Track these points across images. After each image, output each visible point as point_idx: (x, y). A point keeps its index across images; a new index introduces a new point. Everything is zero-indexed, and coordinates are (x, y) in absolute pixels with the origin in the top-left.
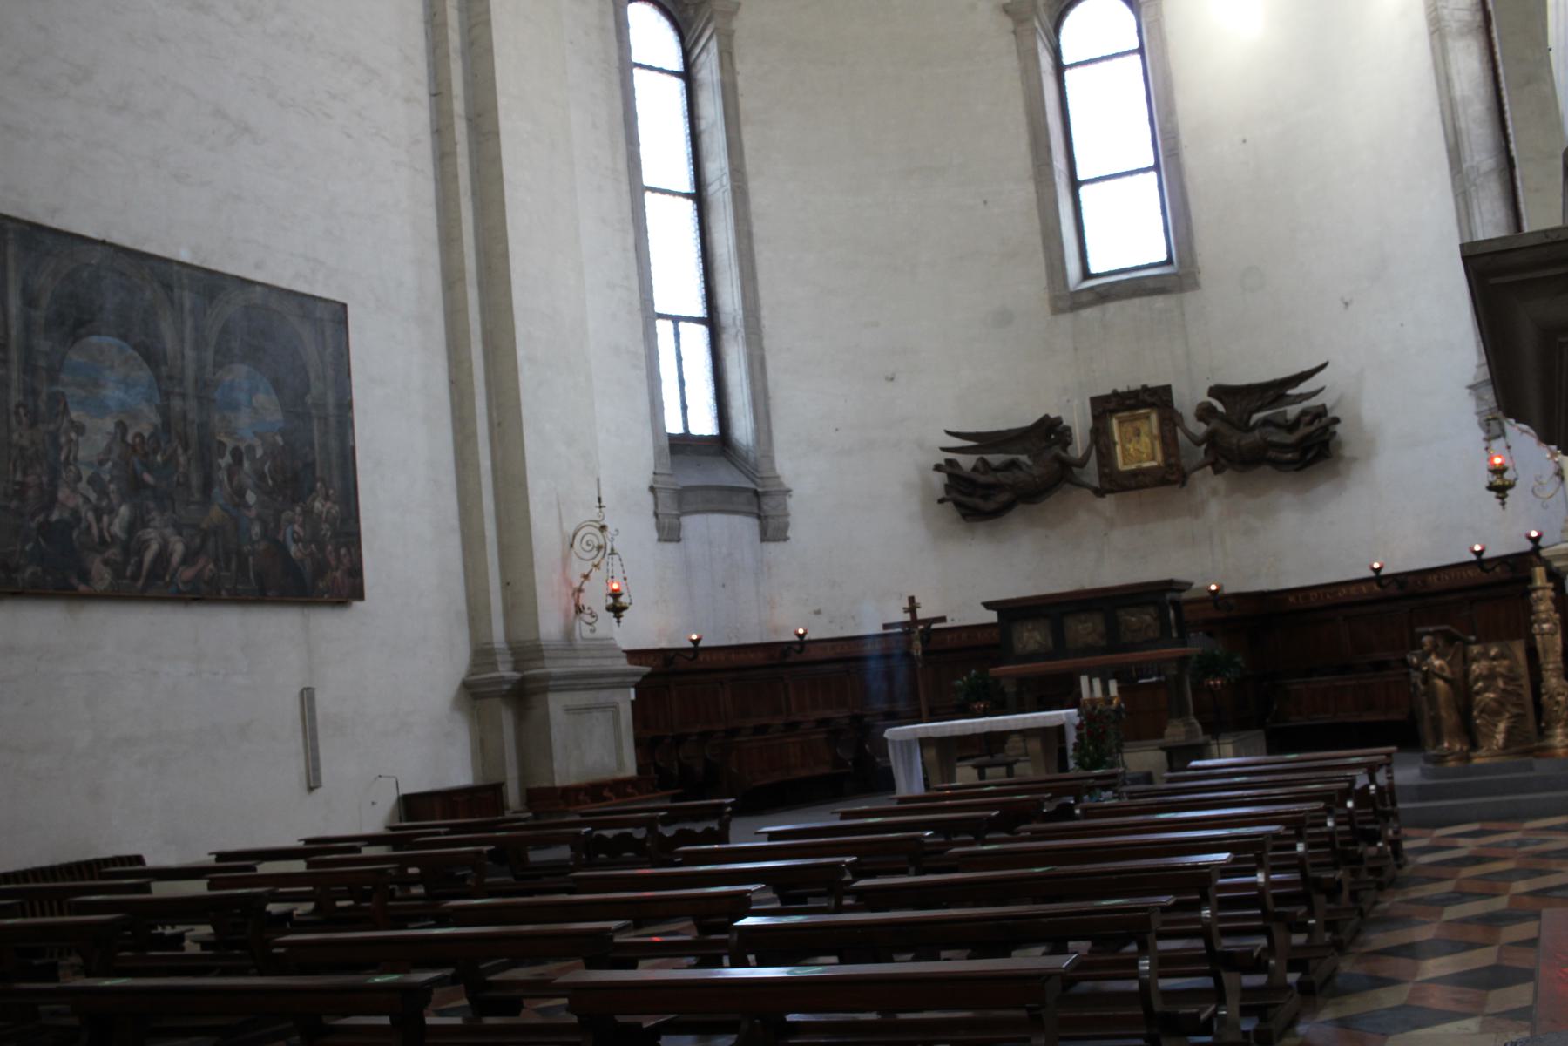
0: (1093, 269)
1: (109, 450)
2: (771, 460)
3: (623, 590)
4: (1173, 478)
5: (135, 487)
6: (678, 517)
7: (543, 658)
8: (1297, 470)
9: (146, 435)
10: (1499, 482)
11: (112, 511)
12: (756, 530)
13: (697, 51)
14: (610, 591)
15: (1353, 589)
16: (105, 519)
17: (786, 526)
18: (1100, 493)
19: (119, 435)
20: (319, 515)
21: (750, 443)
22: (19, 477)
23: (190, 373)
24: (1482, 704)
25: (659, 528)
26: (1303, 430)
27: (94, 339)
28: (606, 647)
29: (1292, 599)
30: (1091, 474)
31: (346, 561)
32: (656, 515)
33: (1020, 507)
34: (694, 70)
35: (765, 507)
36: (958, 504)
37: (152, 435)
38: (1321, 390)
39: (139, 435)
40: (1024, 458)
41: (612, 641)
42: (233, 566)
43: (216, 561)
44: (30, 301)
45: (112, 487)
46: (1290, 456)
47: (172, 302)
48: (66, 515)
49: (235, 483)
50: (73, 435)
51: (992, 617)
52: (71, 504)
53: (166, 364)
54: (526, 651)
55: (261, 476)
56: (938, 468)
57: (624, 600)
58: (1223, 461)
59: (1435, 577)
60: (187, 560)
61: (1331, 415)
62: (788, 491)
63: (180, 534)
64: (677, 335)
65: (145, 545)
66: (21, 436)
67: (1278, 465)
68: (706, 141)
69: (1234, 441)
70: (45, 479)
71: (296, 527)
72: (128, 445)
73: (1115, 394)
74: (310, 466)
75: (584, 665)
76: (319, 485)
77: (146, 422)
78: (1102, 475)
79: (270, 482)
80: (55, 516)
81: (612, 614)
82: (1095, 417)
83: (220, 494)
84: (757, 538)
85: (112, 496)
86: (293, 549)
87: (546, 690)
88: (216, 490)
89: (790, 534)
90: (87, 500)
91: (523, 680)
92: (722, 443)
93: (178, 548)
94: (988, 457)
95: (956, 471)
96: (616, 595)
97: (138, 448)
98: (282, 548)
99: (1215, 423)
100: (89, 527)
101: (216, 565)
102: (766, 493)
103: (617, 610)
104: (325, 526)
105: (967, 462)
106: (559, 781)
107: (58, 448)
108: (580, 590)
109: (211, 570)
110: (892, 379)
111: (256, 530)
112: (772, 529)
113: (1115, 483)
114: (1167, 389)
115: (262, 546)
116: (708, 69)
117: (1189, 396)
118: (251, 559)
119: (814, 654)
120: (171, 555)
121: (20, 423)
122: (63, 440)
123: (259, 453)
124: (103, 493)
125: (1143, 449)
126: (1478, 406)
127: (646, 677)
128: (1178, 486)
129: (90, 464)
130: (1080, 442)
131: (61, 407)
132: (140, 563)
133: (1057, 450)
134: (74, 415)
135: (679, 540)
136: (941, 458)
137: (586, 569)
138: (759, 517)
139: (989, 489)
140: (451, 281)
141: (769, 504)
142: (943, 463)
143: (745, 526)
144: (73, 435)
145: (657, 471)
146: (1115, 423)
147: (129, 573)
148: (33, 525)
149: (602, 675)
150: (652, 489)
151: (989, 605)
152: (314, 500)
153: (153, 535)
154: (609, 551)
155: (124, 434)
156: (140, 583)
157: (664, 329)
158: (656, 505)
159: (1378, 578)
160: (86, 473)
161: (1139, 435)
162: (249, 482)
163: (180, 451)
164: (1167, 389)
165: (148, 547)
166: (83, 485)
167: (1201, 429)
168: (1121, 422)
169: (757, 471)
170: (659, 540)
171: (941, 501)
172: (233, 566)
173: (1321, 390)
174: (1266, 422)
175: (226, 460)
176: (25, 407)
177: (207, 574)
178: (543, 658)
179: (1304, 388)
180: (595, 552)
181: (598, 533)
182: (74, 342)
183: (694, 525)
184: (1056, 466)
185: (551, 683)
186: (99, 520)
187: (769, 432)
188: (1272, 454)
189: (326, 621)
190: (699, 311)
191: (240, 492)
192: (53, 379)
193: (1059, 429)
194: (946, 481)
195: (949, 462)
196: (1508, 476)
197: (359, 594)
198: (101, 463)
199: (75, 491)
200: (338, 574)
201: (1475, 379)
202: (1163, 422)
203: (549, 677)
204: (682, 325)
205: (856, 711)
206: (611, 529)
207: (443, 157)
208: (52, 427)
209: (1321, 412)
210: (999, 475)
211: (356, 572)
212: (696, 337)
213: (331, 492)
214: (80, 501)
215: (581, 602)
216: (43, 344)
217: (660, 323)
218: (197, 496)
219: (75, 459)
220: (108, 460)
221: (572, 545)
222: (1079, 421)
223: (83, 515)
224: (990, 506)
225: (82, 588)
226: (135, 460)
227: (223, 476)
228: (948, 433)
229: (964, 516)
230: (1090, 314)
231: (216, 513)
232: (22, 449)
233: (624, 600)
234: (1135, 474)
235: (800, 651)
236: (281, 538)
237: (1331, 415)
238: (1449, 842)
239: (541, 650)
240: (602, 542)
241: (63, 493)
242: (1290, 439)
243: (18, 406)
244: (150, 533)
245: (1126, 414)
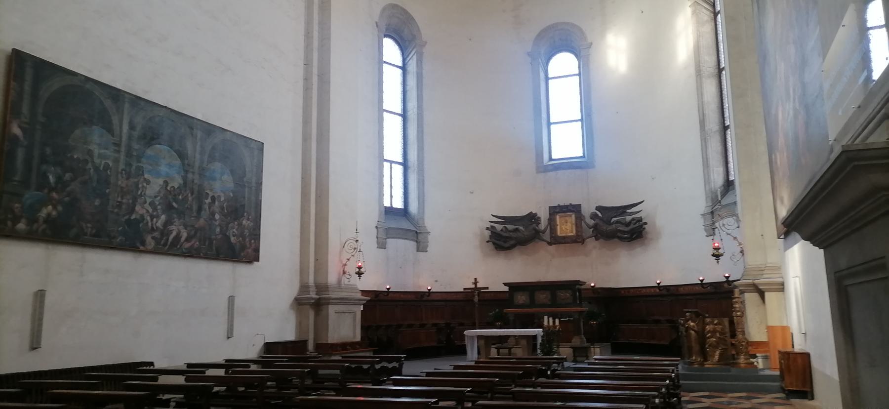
0: (553, 157)
1: (159, 192)
2: (423, 220)
4: (579, 240)
5: (169, 208)
6: (386, 239)
7: (328, 291)
8: (629, 241)
9: (176, 187)
10: (717, 253)
11: (158, 217)
12: (415, 247)
13: (408, 59)
14: (357, 266)
15: (648, 290)
16: (155, 220)
17: (427, 246)
18: (550, 244)
19: (164, 186)
20: (244, 226)
21: (416, 213)
22: (119, 199)
23: (197, 164)
24: (710, 343)
25: (378, 243)
26: (632, 226)
27: (158, 146)
28: (353, 288)
29: (623, 292)
30: (547, 236)
31: (253, 245)
32: (377, 237)
34: (406, 66)
35: (419, 238)
36: (494, 243)
37: (178, 188)
38: (641, 211)
39: (173, 187)
40: (521, 228)
41: (355, 286)
42: (207, 243)
43: (200, 241)
44: (132, 127)
45: (159, 207)
46: (626, 235)
47: (192, 135)
48: (138, 217)
49: (211, 210)
50: (145, 184)
51: (506, 289)
52: (141, 212)
53: (187, 159)
54: (322, 288)
55: (222, 208)
56: (487, 229)
57: (362, 270)
58: (599, 236)
60: (187, 240)
61: (643, 221)
63: (186, 229)
64: (391, 168)
65: (171, 232)
66: (122, 182)
67: (622, 239)
68: (409, 94)
69: (605, 228)
70: (131, 201)
71: (235, 230)
72: (168, 190)
73: (559, 206)
74: (243, 206)
75: (344, 295)
76: (245, 214)
77: (177, 182)
78: (551, 237)
79: (226, 211)
80: (133, 217)
81: (357, 275)
82: (550, 214)
83: (205, 214)
84: (416, 250)
85: (159, 211)
86: (233, 239)
87: (328, 304)
88: (203, 212)
89: (428, 249)
90: (148, 211)
91: (320, 298)
92: (404, 212)
93: (184, 235)
95: (494, 231)
97: (172, 192)
98: (228, 238)
99: (597, 221)
100: (148, 222)
101: (199, 243)
102: (420, 233)
103: (360, 274)
104: (246, 231)
105: (499, 227)
106: (330, 341)
107: (138, 189)
108: (345, 265)
109: (197, 245)
110: (472, 193)
111: (218, 230)
112: (421, 247)
113: (556, 240)
114: (579, 206)
115: (219, 237)
116: (412, 66)
117: (588, 209)
118: (214, 241)
119: (433, 297)
120: (181, 237)
121: (123, 177)
122: (140, 186)
123: (222, 199)
124: (155, 209)
125: (568, 228)
127: (368, 301)
128: (581, 244)
129: (150, 197)
130: (543, 225)
131: (141, 172)
132: (168, 239)
133: (534, 225)
134: (146, 176)
135: (385, 248)
136: (489, 225)
137: (349, 256)
138: (417, 242)
140: (306, 138)
141: (421, 237)
142: (490, 227)
143: (412, 245)
144: (145, 184)
146: (558, 217)
147: (162, 242)
148: (123, 220)
149: (351, 300)
150: (377, 227)
151: (505, 284)
152: (243, 220)
153: (174, 228)
154: (358, 250)
155: (167, 186)
156: (167, 247)
157: (386, 165)
158: (378, 234)
159: (659, 286)
160: (149, 200)
161: (567, 223)
162: (217, 210)
163: (190, 195)
164: (579, 206)
165: (172, 233)
166: (147, 205)
167: (591, 222)
168: (560, 217)
169: (418, 224)
170: (377, 248)
171: (487, 242)
172: (207, 243)
173: (641, 211)
174: (617, 222)
175: (209, 200)
176: (125, 171)
177: (196, 246)
178: (328, 291)
179: (633, 210)
180: (353, 250)
181: (355, 242)
182: (149, 147)
183: (391, 243)
184: (534, 232)
185: (331, 301)
186: (152, 220)
187: (424, 209)
188: (619, 234)
189: (242, 269)
190: (400, 160)
191: (213, 214)
192: (139, 161)
193: (536, 217)
194: (490, 234)
196: (721, 251)
197: (257, 259)
198: (156, 197)
199: (143, 208)
200: (250, 251)
201: (704, 211)
202: (576, 218)
203: (330, 299)
204: (393, 165)
205: (448, 322)
206: (360, 241)
207: (307, 89)
208: (136, 180)
209: (640, 220)
210: (511, 233)
211: (257, 250)
212: (398, 170)
213: (250, 217)
214: (145, 211)
215: (345, 270)
216: (136, 146)
218: (195, 214)
219: (145, 194)
220: (159, 196)
221: (344, 247)
223: (145, 217)
224: (507, 245)
225: (142, 248)
226: (170, 197)
227: (206, 207)
228: (492, 215)
229: (496, 248)
230: (551, 174)
231: (202, 222)
232: (122, 188)
233: (362, 270)
234: (564, 237)
235: (428, 296)
236: (228, 234)
237: (643, 221)
238: (697, 399)
239: (328, 287)
240: (356, 247)
241: (138, 208)
242: (626, 229)
243: (122, 170)
244: (173, 227)
245: (563, 214)
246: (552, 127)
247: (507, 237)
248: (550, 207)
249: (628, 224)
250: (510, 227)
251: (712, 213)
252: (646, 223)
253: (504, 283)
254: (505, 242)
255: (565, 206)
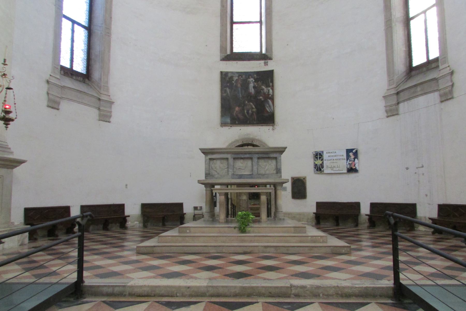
3: (12, 109)
25: (49, 100)
57: (11, 116)
62: (114, 102)
64: (73, 31)
81: (3, 122)
89: (111, 120)
96: (7, 112)
126: (385, 103)
143: (93, 113)
145: (51, 75)
170: (48, 106)
217: (64, 20)
246: (235, 26)
251: (398, 93)
253: (201, 149)
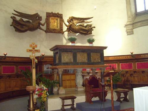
30: (44, 28)
33: (28, 32)
36: (14, 27)
46: (84, 32)
56: (11, 17)
59: (111, 58)
82: (47, 16)
94: (23, 19)
105: (18, 18)
114: (62, 15)
130: (43, 21)
133: (39, 21)
139: (22, 25)
146: (51, 18)
161: (55, 22)
167: (67, 24)
171: (11, 25)
174: (80, 25)
179: (88, 21)
184: (38, 24)
195: (14, 17)
209: (91, 26)
222: (44, 16)
224: (23, 29)
228: (14, 10)
234: (54, 30)
245: (53, 17)
247: (24, 25)
248: (46, 13)
249: (86, 27)
250: (25, 20)
252: (94, 27)
254: (23, 27)
255: (55, 13)
